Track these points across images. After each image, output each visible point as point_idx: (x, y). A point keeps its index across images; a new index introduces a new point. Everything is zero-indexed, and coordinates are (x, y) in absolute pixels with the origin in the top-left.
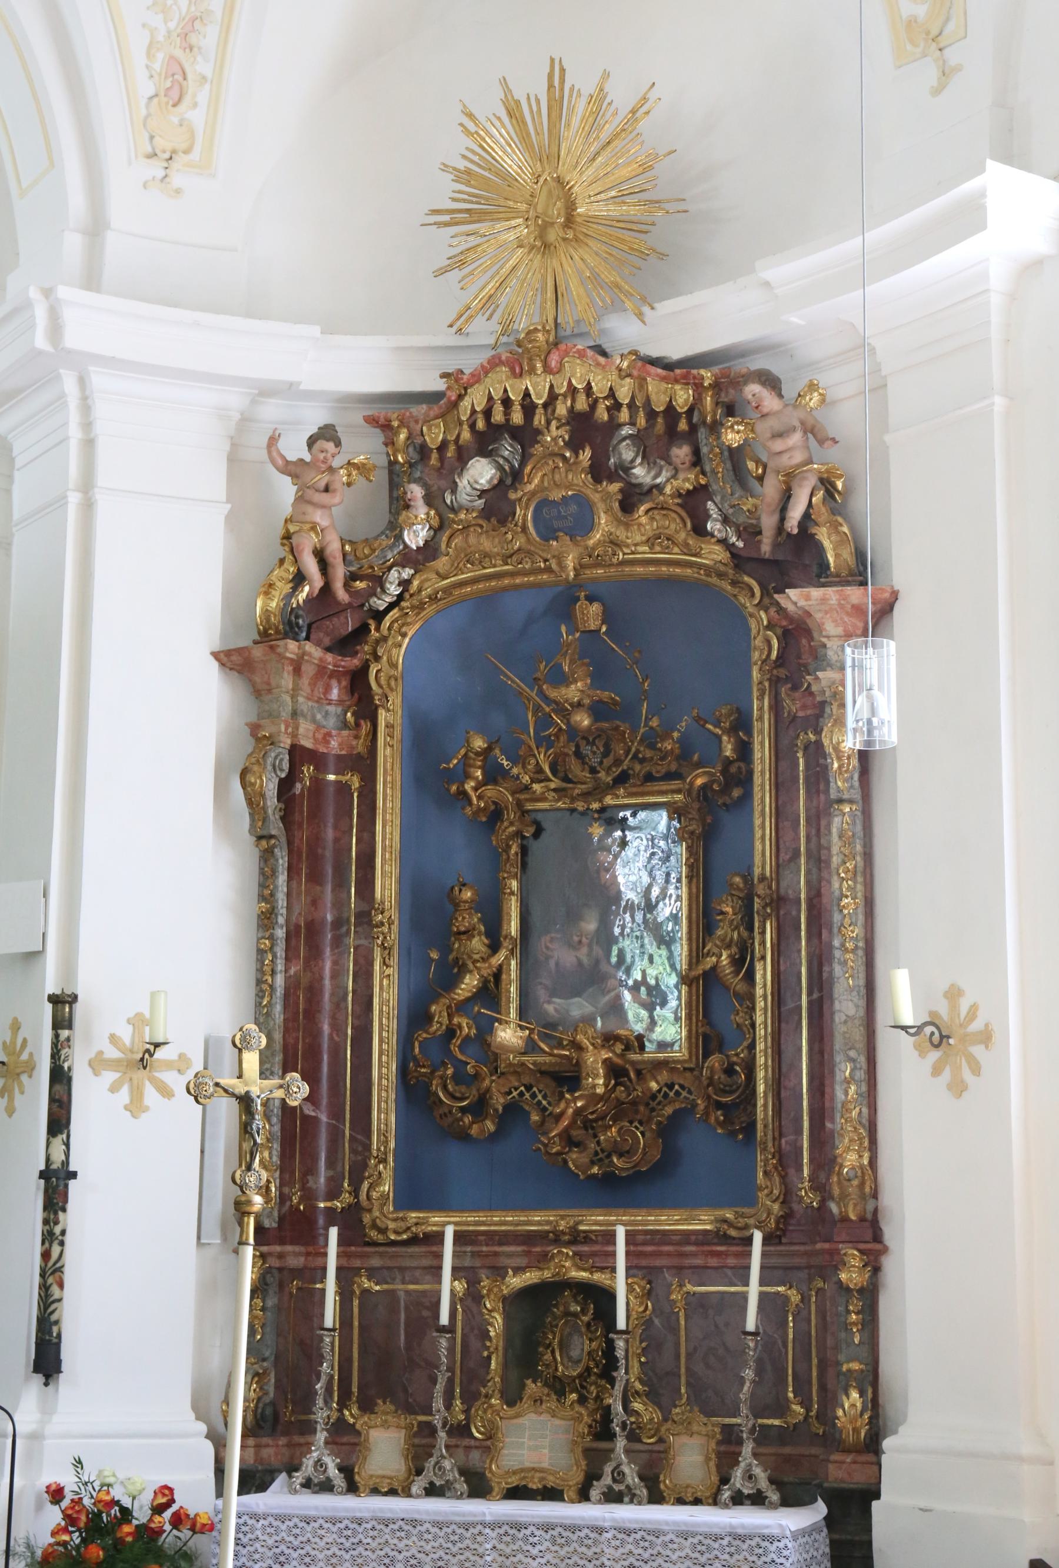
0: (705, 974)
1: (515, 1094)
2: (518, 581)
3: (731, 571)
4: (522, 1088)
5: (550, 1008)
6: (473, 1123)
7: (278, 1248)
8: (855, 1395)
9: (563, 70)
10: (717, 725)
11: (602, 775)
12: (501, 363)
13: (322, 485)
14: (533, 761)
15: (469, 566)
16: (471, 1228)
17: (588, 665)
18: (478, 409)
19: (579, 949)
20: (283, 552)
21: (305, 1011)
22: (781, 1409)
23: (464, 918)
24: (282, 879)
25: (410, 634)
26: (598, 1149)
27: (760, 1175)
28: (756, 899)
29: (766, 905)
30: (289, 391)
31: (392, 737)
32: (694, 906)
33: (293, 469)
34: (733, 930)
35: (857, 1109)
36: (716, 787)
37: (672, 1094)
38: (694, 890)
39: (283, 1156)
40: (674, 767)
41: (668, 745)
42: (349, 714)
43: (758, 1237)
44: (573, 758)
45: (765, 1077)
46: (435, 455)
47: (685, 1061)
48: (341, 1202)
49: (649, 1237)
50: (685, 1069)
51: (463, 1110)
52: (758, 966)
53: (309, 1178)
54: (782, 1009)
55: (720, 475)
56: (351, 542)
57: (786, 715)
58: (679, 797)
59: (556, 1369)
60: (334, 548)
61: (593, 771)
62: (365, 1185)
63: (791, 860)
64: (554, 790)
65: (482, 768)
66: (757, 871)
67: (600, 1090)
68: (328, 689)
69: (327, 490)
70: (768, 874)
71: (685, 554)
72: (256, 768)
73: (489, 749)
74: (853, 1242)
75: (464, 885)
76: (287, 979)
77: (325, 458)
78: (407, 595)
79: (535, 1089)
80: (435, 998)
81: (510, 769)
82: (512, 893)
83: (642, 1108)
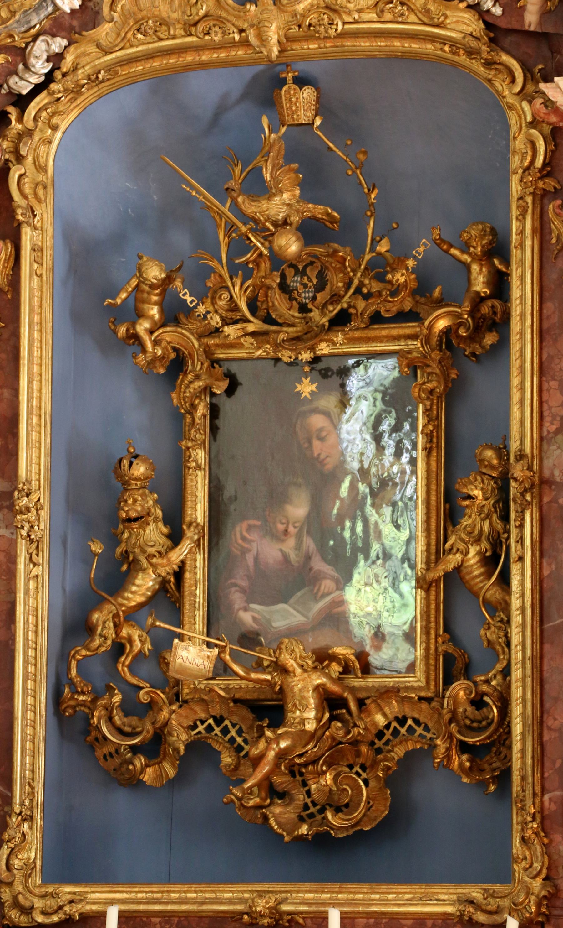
0: (447, 576)
1: (201, 728)
2: (204, 58)
3: (484, 48)
4: (211, 721)
6: (147, 766)
10: (465, 248)
11: (315, 314)
14: (226, 295)
15: (139, 36)
16: (142, 907)
17: (297, 171)
19: (283, 541)
23: (135, 501)
25: (63, 127)
26: (308, 801)
27: (517, 841)
28: (513, 484)
29: (526, 490)
31: (40, 264)
32: (433, 487)
34: (483, 520)
36: (462, 332)
37: (403, 731)
38: (434, 466)
40: (408, 305)
41: (400, 278)
44: (277, 291)
45: (523, 714)
47: (420, 688)
50: (421, 699)
51: (134, 749)
52: (515, 569)
54: (546, 626)
57: (554, 241)
61: (304, 309)
64: (253, 334)
65: (160, 304)
66: (514, 446)
70: (528, 450)
71: (425, 24)
73: (169, 279)
75: (136, 457)
78: (58, 75)
79: (227, 722)
80: (99, 602)
81: (195, 307)
83: (364, 749)
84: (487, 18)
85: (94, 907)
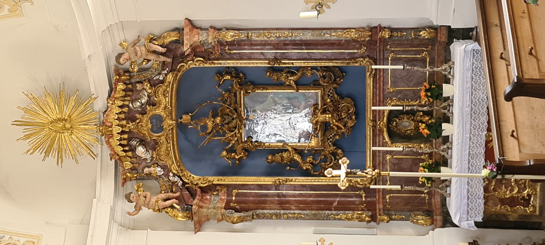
0: (296, 84)
2: (175, 140)
3: (176, 72)
4: (329, 141)
7: (378, 210)
8: (421, 33)
9: (16, 121)
10: (220, 80)
12: (108, 141)
13: (144, 199)
14: (230, 137)
15: (170, 155)
17: (202, 118)
18: (122, 149)
20: (164, 212)
21: (306, 204)
22: (424, 60)
23: (277, 159)
24: (266, 211)
25: (190, 174)
26: (347, 118)
27: (356, 65)
29: (277, 62)
30: (113, 209)
32: (275, 88)
33: (138, 208)
34: (283, 75)
35: (339, 33)
37: (331, 95)
38: (270, 88)
39: (350, 210)
40: (233, 94)
42: (215, 193)
43: (374, 67)
44: (229, 125)
45: (328, 63)
46: (135, 165)
48: (363, 194)
49: (374, 99)
50: (324, 90)
53: (356, 203)
54: (308, 58)
55: (146, 75)
58: (242, 92)
59: (412, 129)
60: (163, 196)
61: (233, 119)
62: (358, 186)
64: (239, 131)
68: (207, 199)
69: (145, 197)
70: (268, 62)
71: (170, 86)
72: (232, 219)
73: (226, 150)
74: (377, 34)
75: (267, 159)
76: (296, 210)
77: (136, 197)
78: (178, 174)
83: (335, 104)
84: (169, 72)
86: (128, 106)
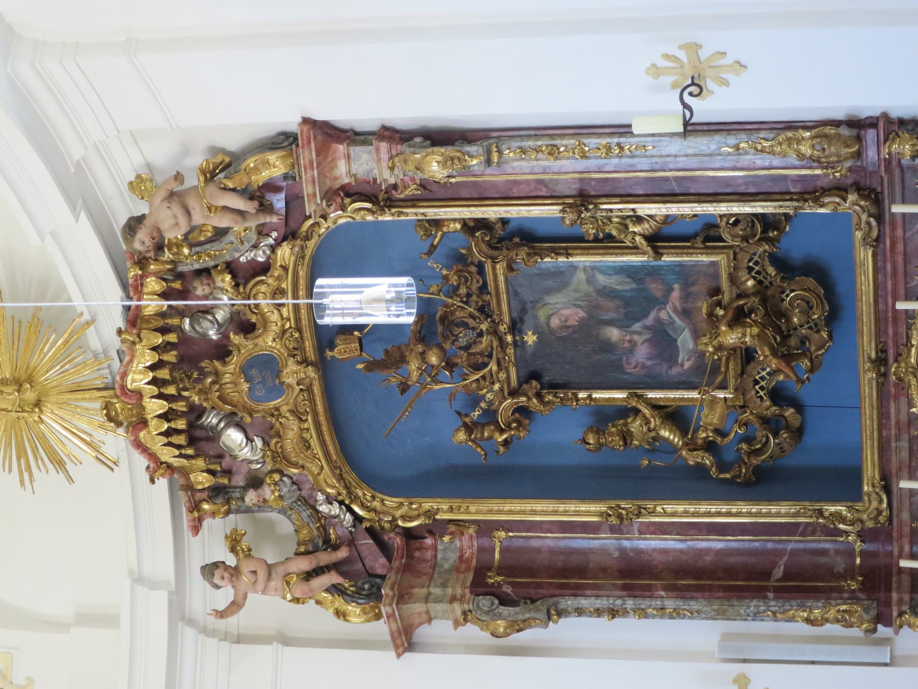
1: (762, 393)
4: (757, 387)
5: (687, 365)
16: (876, 443)
19: (635, 342)
27: (822, 211)
35: (762, 141)
37: (757, 268)
40: (473, 269)
47: (728, 258)
48: (855, 542)
49: (880, 300)
50: (735, 259)
53: (836, 571)
54: (678, 191)
56: (299, 544)
57: (419, 192)
61: (481, 334)
63: (546, 186)
67: (756, 330)
79: (757, 377)
81: (482, 409)
82: (590, 397)
84: (280, 240)
85: (877, 472)
86: (179, 329)
